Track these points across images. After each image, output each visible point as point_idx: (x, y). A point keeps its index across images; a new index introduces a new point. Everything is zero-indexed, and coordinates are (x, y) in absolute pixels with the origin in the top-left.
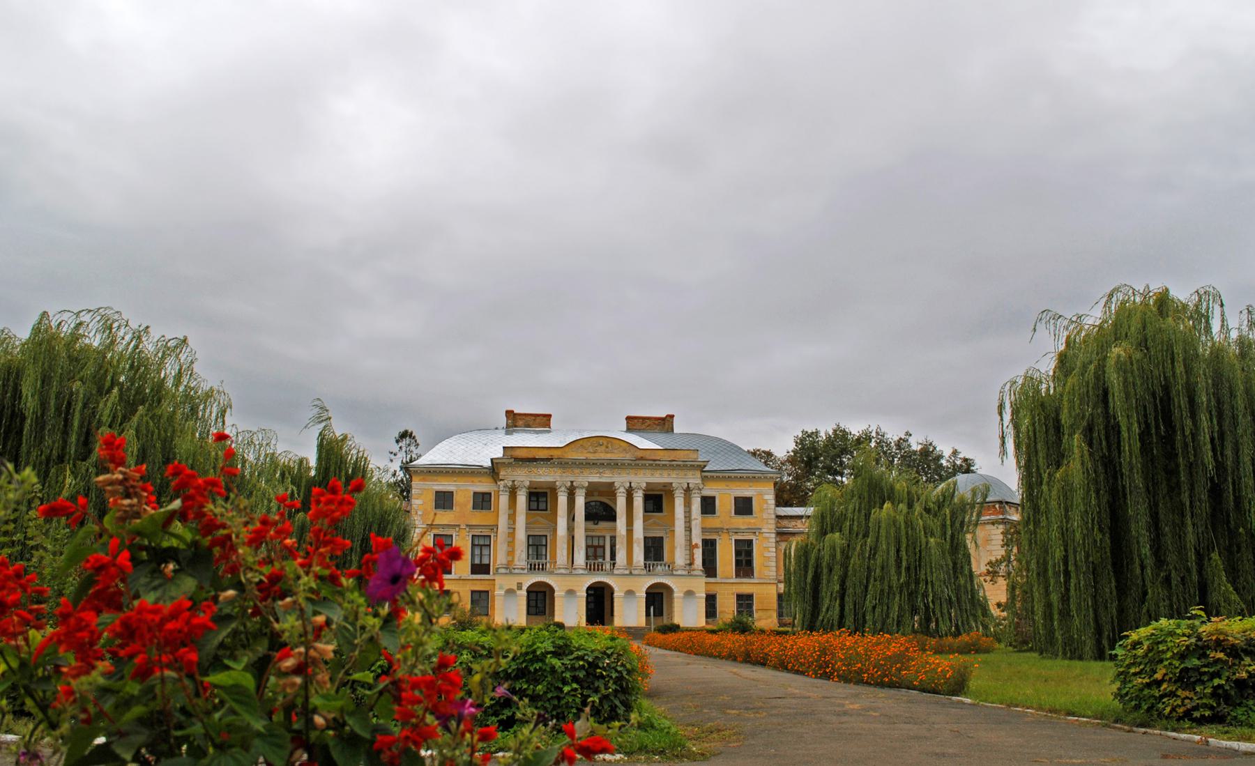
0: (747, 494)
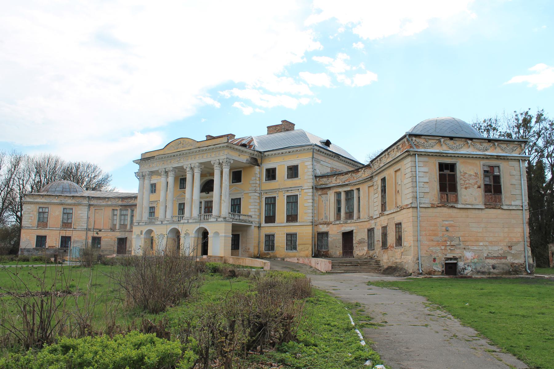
0: (294, 163)
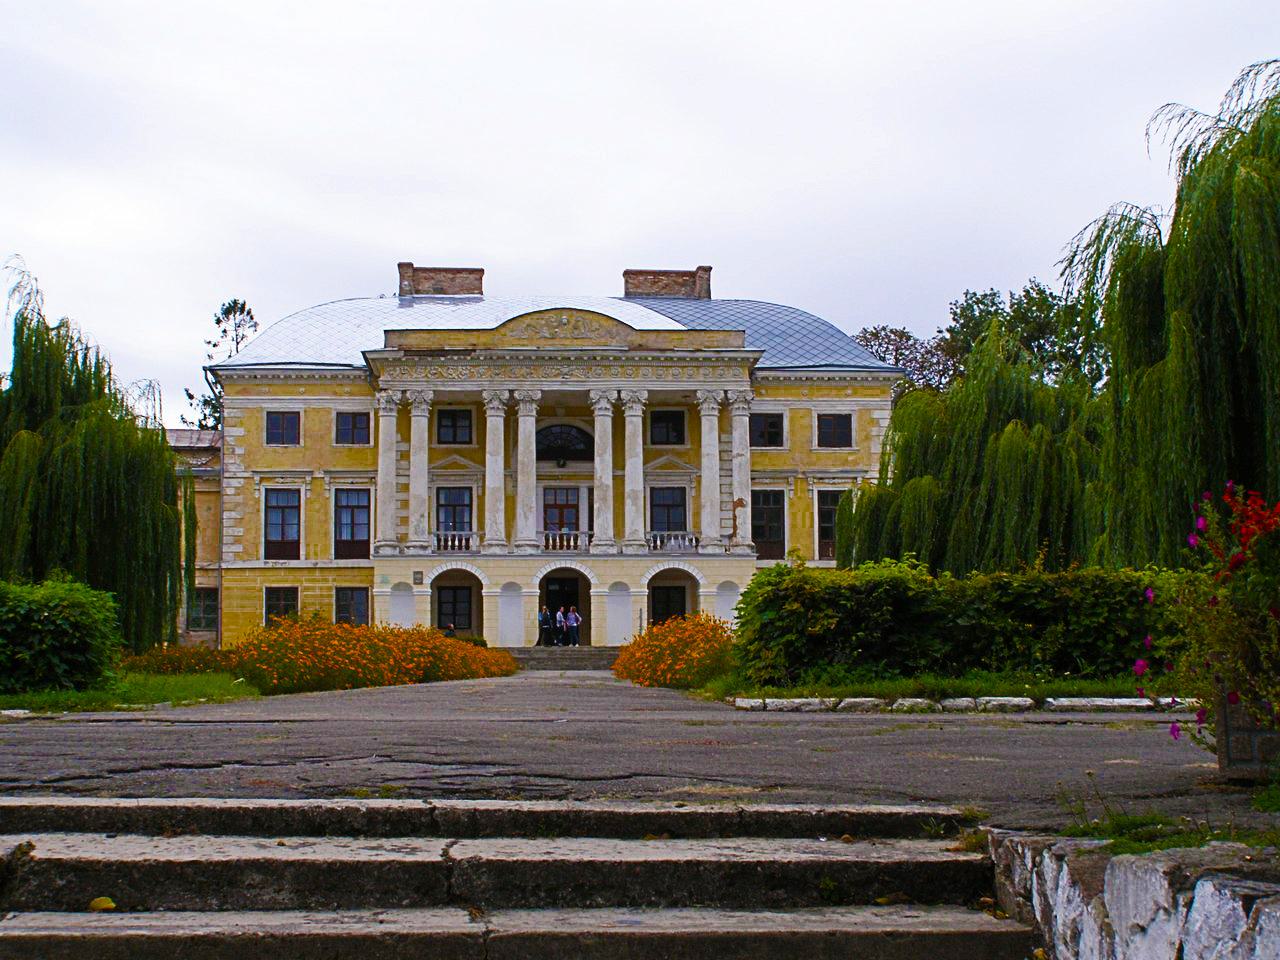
0: (841, 408)
